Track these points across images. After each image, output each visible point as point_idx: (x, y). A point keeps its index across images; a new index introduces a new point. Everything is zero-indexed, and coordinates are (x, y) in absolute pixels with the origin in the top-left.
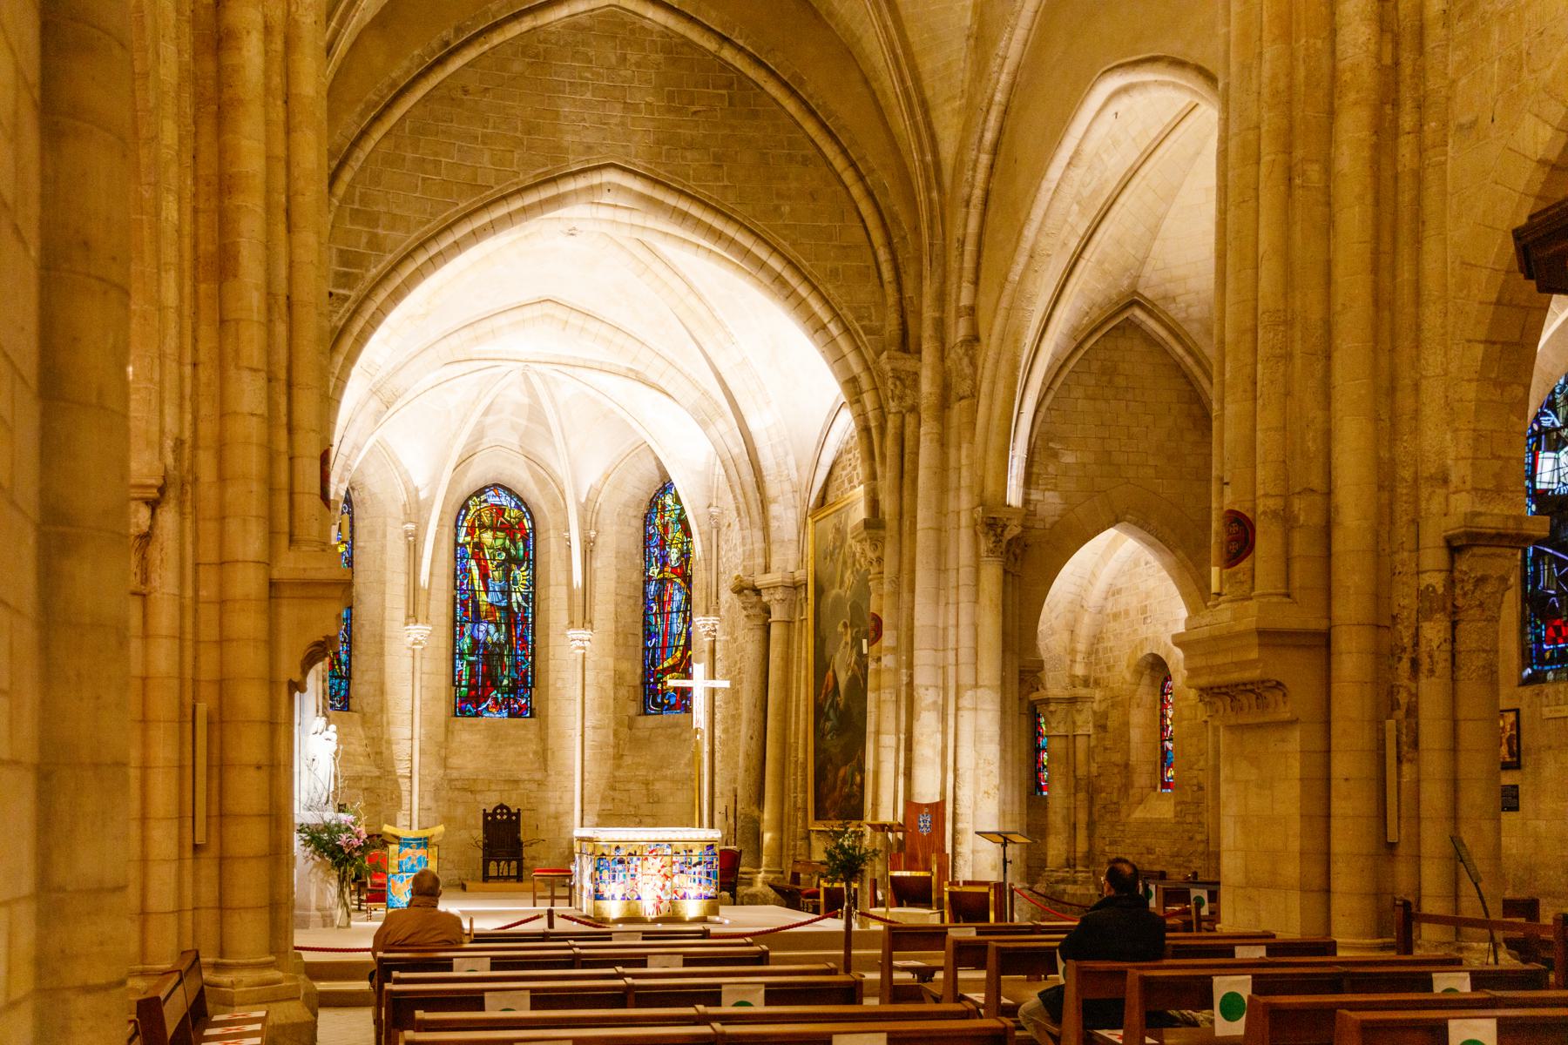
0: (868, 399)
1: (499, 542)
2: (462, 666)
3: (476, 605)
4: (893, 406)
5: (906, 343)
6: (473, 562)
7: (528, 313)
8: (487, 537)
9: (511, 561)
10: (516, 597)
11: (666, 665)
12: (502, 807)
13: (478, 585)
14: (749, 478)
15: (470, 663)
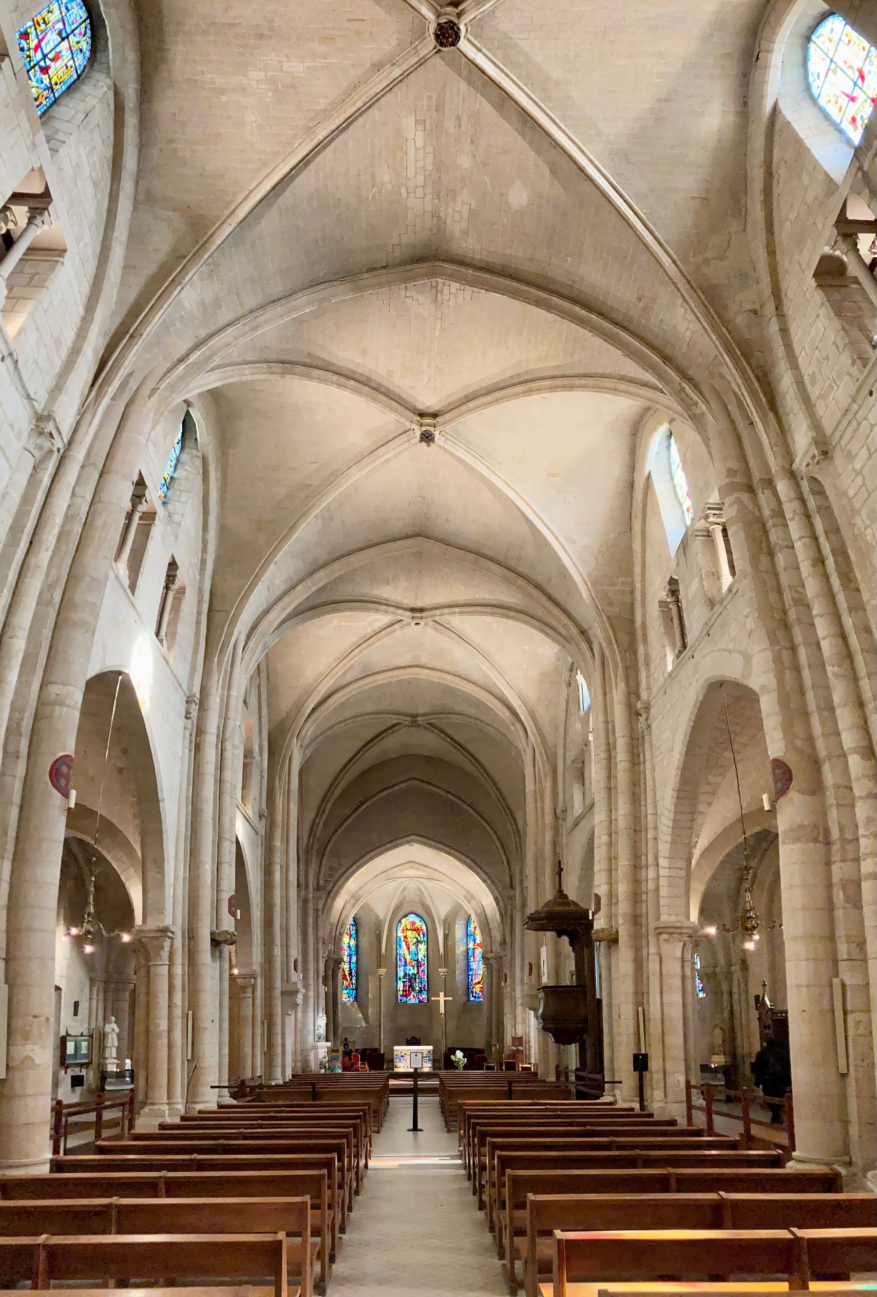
0: (501, 903)
1: (413, 936)
2: (400, 985)
3: (405, 959)
4: (509, 907)
5: (512, 886)
6: (403, 944)
7: (404, 866)
8: (409, 933)
9: (418, 942)
10: (420, 956)
11: (477, 981)
12: (414, 1037)
13: (406, 952)
14: (485, 921)
15: (404, 982)
